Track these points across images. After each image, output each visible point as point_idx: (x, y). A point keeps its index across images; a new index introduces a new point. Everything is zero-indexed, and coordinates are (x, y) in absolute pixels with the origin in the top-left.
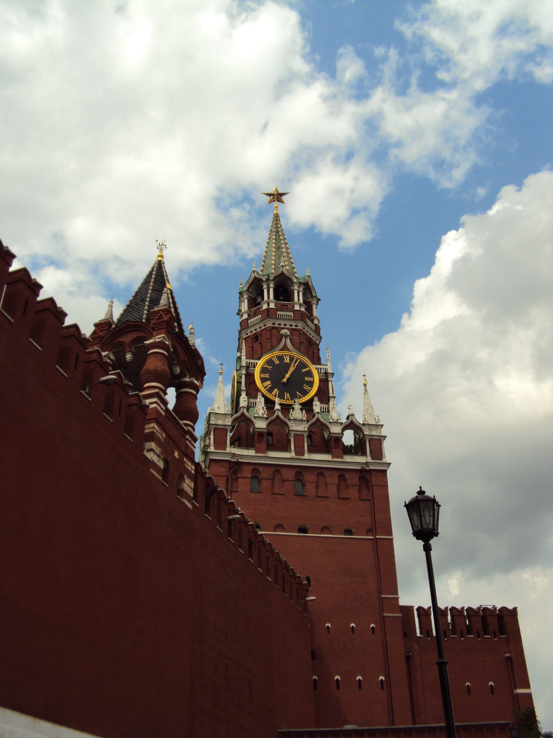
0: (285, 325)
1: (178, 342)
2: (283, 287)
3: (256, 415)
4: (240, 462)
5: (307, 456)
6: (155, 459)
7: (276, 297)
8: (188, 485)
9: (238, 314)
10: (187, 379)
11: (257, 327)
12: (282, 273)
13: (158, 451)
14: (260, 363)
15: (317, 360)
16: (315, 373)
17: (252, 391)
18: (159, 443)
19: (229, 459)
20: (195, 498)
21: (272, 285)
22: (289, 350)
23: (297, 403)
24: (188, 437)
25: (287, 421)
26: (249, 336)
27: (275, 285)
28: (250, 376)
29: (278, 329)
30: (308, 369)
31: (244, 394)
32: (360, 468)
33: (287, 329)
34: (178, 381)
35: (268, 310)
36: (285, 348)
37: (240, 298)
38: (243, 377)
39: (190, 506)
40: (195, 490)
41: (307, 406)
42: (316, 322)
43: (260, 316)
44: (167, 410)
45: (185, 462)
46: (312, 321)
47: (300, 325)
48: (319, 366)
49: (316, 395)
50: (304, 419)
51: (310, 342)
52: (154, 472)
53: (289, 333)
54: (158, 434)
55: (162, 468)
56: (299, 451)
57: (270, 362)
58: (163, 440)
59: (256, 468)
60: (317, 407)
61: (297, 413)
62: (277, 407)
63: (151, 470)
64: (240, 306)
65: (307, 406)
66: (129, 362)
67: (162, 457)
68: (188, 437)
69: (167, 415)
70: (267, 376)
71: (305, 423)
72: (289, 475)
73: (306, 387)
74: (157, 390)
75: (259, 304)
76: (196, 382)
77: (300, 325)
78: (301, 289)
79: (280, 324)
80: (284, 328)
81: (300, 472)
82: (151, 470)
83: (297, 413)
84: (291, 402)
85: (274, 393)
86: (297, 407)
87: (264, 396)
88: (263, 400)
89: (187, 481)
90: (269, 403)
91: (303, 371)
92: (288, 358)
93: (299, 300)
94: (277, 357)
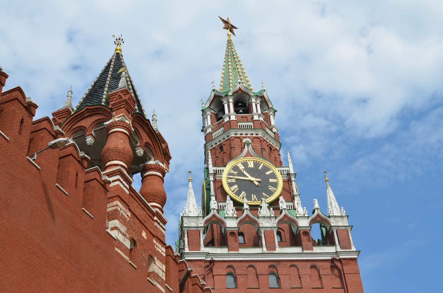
0: (246, 134)
1: (140, 125)
2: (242, 104)
3: (226, 216)
4: (214, 261)
5: (278, 250)
6: (120, 237)
7: (237, 111)
8: (158, 268)
9: (202, 131)
10: (152, 162)
11: (221, 138)
12: (240, 89)
13: (123, 229)
14: (227, 169)
16: (278, 174)
18: (123, 221)
19: (204, 258)
21: (231, 100)
22: (251, 156)
23: (263, 202)
24: (155, 218)
25: (256, 219)
26: (214, 148)
27: (234, 100)
29: (240, 139)
30: (271, 172)
31: (213, 198)
32: (330, 258)
33: (249, 137)
34: (143, 165)
35: (229, 122)
36: (248, 154)
37: (203, 115)
38: (212, 183)
39: (163, 290)
40: (167, 273)
41: (274, 204)
43: (223, 128)
44: (131, 189)
45: (154, 244)
46: (271, 130)
48: (282, 169)
49: (280, 195)
50: (273, 215)
51: (271, 149)
52: (119, 251)
53: (250, 141)
54: (122, 211)
55: (129, 248)
56: (271, 247)
58: (128, 219)
59: (230, 265)
60: (283, 204)
61: (264, 211)
62: (246, 206)
63: (116, 249)
64: (204, 123)
65: (274, 204)
66: (90, 145)
67: (128, 236)
68: (155, 218)
69: (132, 193)
71: (273, 220)
72: (262, 269)
73: (271, 188)
74: (119, 167)
75: (221, 118)
76: (161, 164)
77: (260, 134)
78: (259, 102)
79: (241, 134)
80: (246, 137)
81: (274, 266)
82: (116, 249)
83: (264, 211)
84: (257, 203)
85: (241, 196)
86: (265, 206)
87: (232, 199)
88: (232, 202)
89: (158, 263)
90: (238, 205)
91: (267, 173)
92: (252, 162)
93: (257, 112)
94: (242, 163)
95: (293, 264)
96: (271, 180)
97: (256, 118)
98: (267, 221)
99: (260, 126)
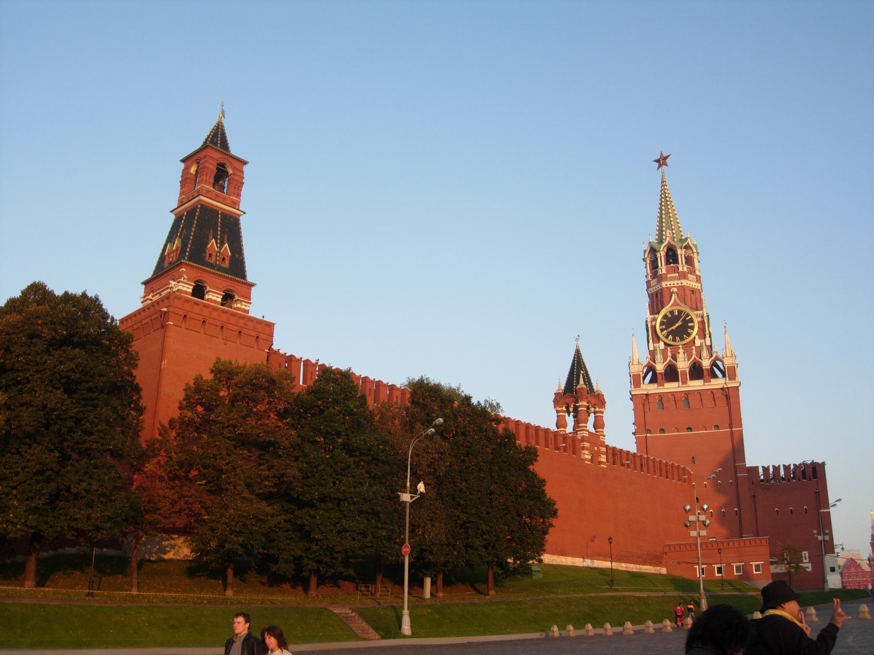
6: (586, 457)
7: (668, 263)
8: (603, 458)
10: (597, 409)
15: (698, 305)
17: (657, 339)
18: (587, 449)
20: (607, 461)
22: (678, 305)
28: (654, 327)
29: (669, 289)
42: (697, 273)
47: (685, 282)
57: (665, 317)
70: (664, 327)
73: (690, 331)
77: (685, 282)
83: (681, 356)
86: (681, 351)
95: (700, 392)
96: (690, 324)
97: (681, 269)
98: (683, 365)
99: (683, 276)
